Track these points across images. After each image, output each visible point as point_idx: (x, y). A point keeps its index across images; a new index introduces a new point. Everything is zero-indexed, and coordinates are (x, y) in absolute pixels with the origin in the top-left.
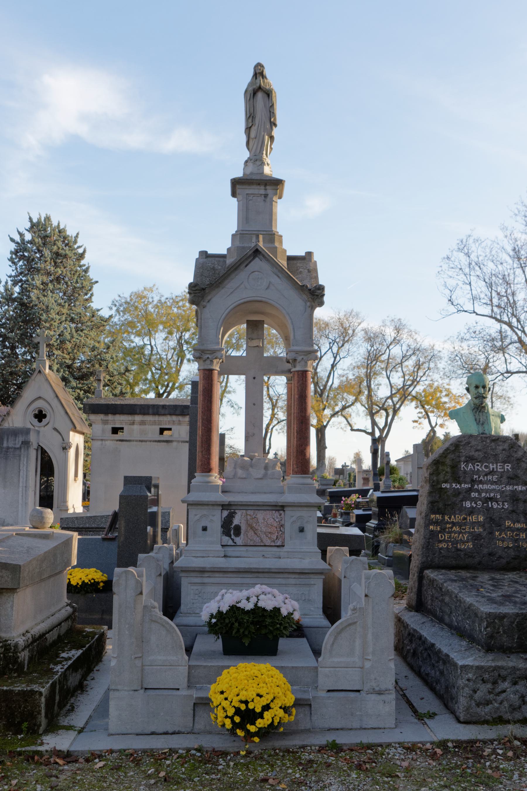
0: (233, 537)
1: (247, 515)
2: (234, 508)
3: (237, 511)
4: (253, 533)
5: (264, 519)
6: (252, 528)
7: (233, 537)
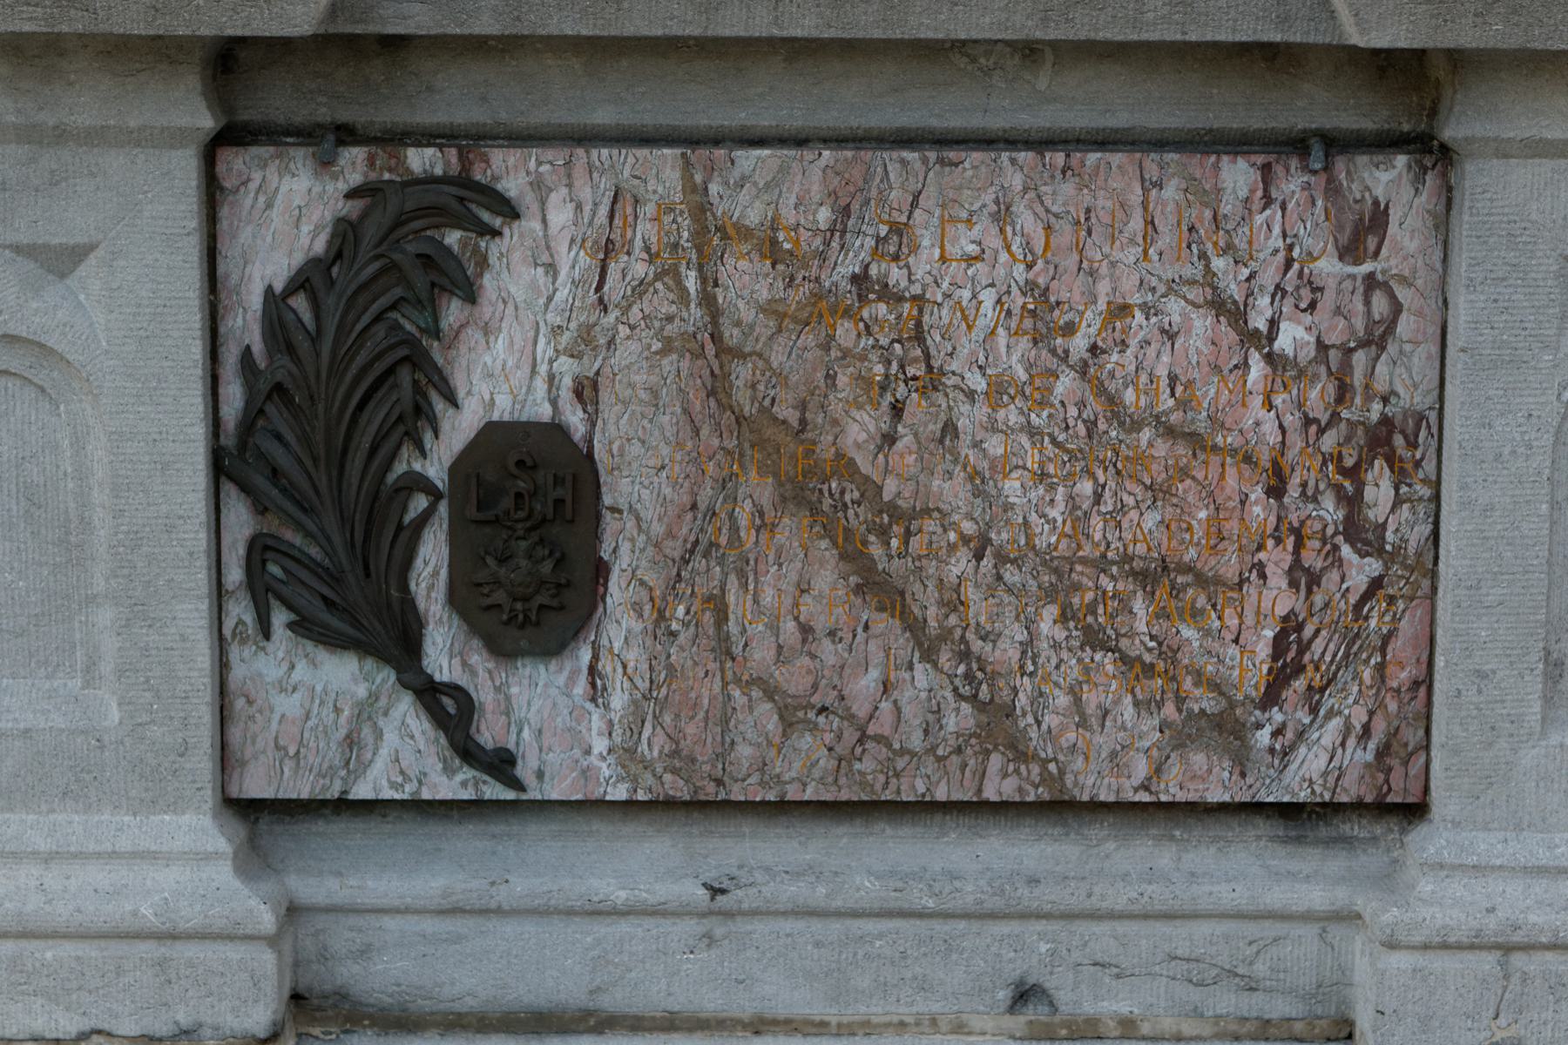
0: (445, 651)
1: (710, 235)
2: (454, 99)
3: (511, 171)
4: (827, 577)
5: (1041, 317)
6: (813, 486)
7: (445, 651)
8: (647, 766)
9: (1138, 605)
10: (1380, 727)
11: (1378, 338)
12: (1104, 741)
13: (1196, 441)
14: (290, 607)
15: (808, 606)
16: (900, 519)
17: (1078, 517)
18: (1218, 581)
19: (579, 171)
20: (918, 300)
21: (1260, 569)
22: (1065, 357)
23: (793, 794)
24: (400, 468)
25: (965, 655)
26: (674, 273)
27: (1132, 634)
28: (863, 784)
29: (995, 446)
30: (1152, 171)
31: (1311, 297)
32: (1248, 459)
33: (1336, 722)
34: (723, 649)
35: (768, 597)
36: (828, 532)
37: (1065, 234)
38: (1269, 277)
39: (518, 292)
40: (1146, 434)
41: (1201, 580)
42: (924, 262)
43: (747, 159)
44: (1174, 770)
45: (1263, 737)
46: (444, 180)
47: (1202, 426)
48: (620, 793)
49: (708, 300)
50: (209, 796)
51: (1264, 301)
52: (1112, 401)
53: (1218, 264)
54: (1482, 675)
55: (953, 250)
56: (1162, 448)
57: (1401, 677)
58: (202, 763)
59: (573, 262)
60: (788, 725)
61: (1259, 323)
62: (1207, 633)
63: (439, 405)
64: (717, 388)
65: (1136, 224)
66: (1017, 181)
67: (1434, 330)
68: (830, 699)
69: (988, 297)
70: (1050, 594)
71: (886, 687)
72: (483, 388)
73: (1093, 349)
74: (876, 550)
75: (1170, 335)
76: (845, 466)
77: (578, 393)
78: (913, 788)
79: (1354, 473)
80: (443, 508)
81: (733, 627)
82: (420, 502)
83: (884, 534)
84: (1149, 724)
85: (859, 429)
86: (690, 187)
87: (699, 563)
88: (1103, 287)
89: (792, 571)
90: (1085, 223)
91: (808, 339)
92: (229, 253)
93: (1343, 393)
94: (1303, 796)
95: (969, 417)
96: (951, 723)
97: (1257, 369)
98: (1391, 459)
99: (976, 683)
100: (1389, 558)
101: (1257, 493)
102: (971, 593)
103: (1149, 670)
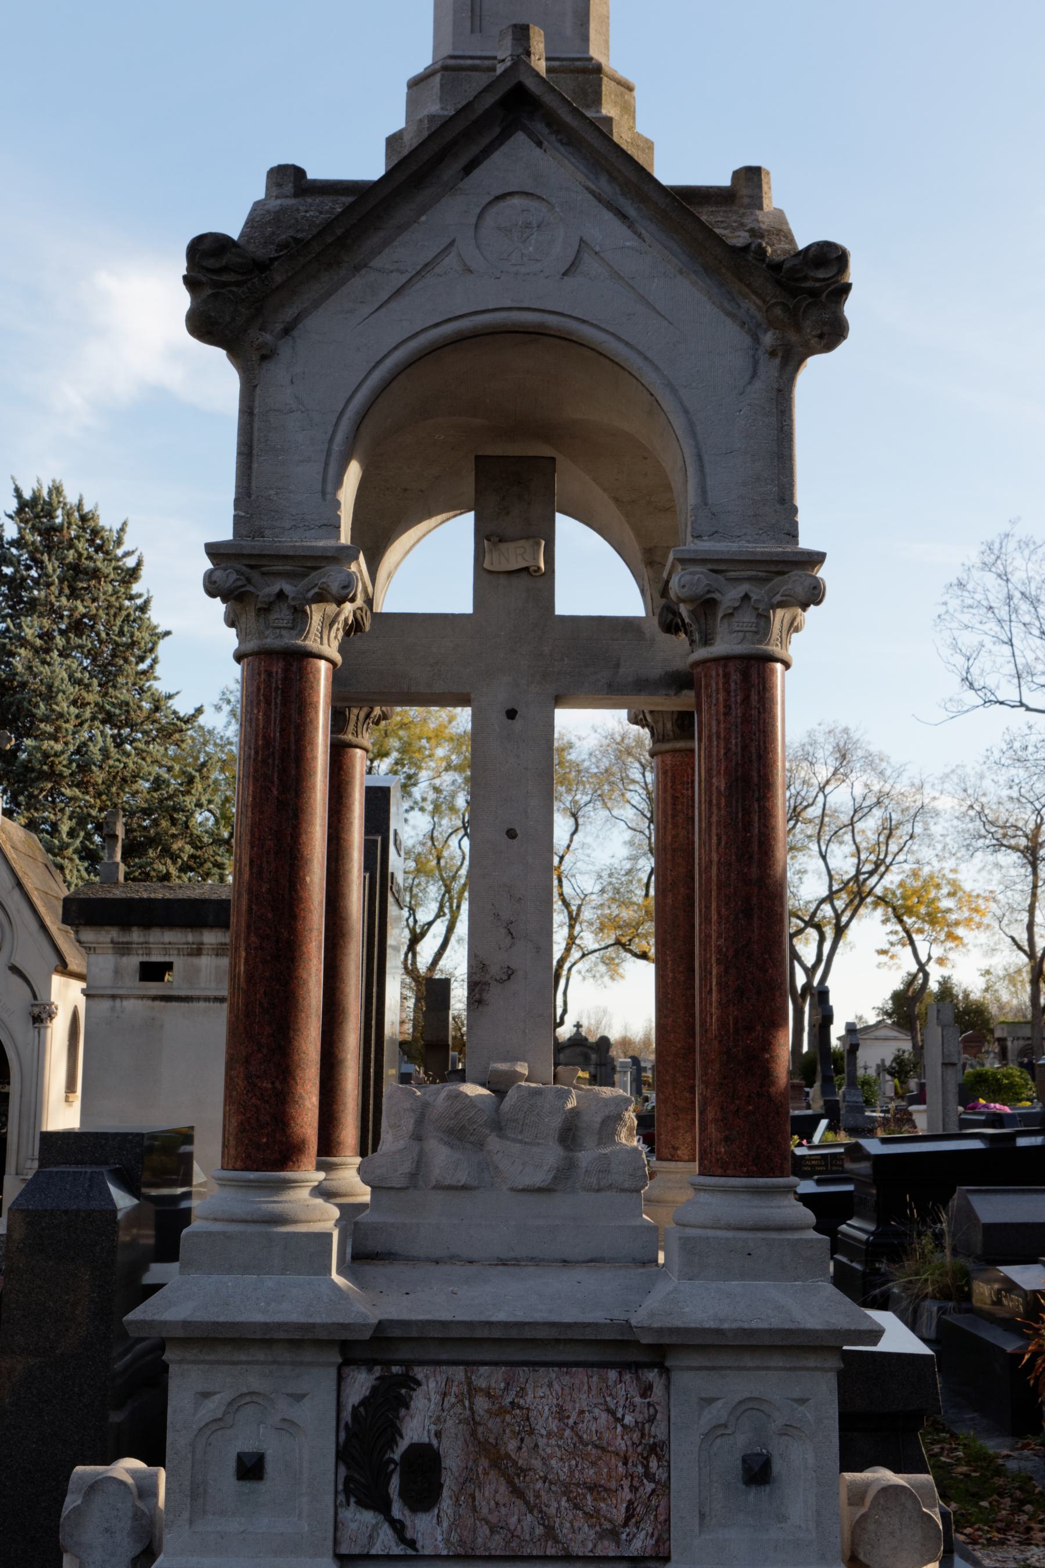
0: (398, 1510)
1: (472, 1391)
2: (405, 1353)
3: (419, 1372)
4: (503, 1488)
5: (561, 1414)
6: (499, 1461)
7: (398, 1510)
8: (453, 1544)
9: (588, 1497)
10: (656, 1533)
11: (652, 1419)
12: (580, 1537)
13: (603, 1449)
14: (356, 1497)
15: (498, 1497)
16: (523, 1471)
17: (572, 1472)
18: (610, 1490)
19: (437, 1373)
20: (528, 1409)
21: (622, 1486)
22: (567, 1425)
23: (493, 1553)
24: (387, 1456)
25: (541, 1512)
26: (462, 1401)
27: (587, 1505)
28: (513, 1550)
29: (549, 1450)
30: (590, 1373)
31: (633, 1407)
32: (617, 1454)
33: (644, 1532)
34: (474, 1509)
35: (487, 1494)
36: (503, 1475)
37: (567, 1391)
38: (622, 1403)
39: (420, 1407)
40: (590, 1447)
41: (606, 1490)
42: (529, 1398)
43: (484, 1370)
44: (599, 1546)
45: (624, 1536)
46: (401, 1375)
47: (605, 1445)
48: (445, 1553)
49: (471, 1409)
50: (331, 1552)
51: (620, 1410)
52: (580, 1438)
53: (608, 1399)
54: (682, 1518)
55: (537, 1395)
56: (594, 1451)
57: (661, 1518)
58: (330, 1543)
59: (435, 1398)
60: (492, 1532)
61: (619, 1415)
62: (607, 1505)
63: (398, 1438)
64: (474, 1434)
65: (586, 1388)
66: (554, 1376)
67: (666, 1418)
68: (504, 1525)
69: (546, 1408)
70: (564, 1493)
71: (519, 1521)
72: (410, 1434)
73: (575, 1423)
74: (516, 1481)
75: (596, 1419)
76: (508, 1456)
77: (436, 1435)
78: (527, 1551)
79: (647, 1459)
80: (398, 1468)
81: (477, 1503)
82: (392, 1466)
83: (519, 1476)
84: (592, 1532)
85: (512, 1445)
86: (467, 1377)
87: (468, 1484)
88: (577, 1405)
89: (493, 1487)
90: (572, 1388)
91: (498, 1420)
92: (343, 1395)
93: (643, 1436)
94: (635, 1554)
95: (542, 1442)
96: (537, 1532)
97: (619, 1428)
98: (657, 1455)
99: (544, 1519)
100: (657, 1483)
101: (620, 1464)
102: (542, 1493)
103: (592, 1516)
